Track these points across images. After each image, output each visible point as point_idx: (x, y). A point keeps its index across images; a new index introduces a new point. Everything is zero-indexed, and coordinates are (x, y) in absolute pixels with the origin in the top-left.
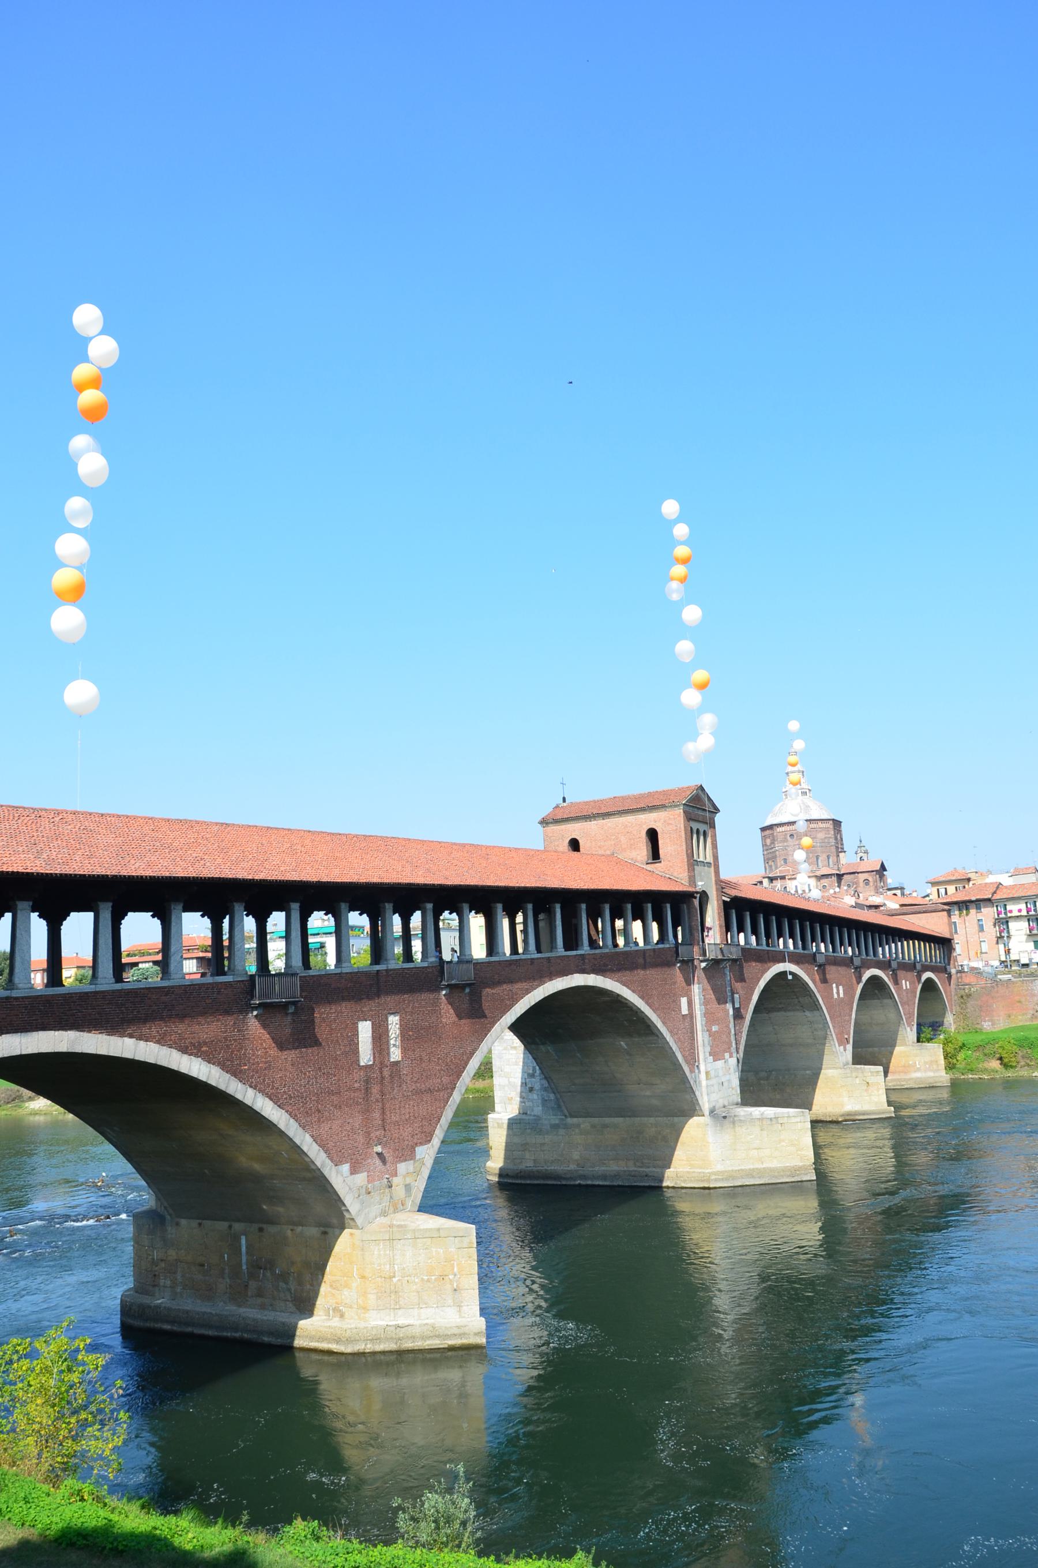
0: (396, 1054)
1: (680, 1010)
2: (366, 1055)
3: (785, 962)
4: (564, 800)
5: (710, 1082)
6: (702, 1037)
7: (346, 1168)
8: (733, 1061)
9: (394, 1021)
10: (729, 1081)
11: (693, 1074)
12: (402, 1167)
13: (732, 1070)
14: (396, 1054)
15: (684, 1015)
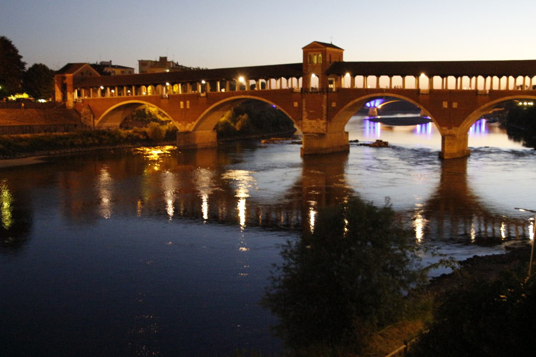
0: (188, 107)
1: (293, 105)
2: (182, 107)
3: (383, 93)
4: (331, 43)
5: (306, 125)
6: (305, 113)
7: (177, 122)
8: (324, 121)
9: (188, 102)
10: (319, 127)
11: (298, 123)
12: (189, 124)
13: (321, 124)
14: (188, 107)
15: (295, 107)
